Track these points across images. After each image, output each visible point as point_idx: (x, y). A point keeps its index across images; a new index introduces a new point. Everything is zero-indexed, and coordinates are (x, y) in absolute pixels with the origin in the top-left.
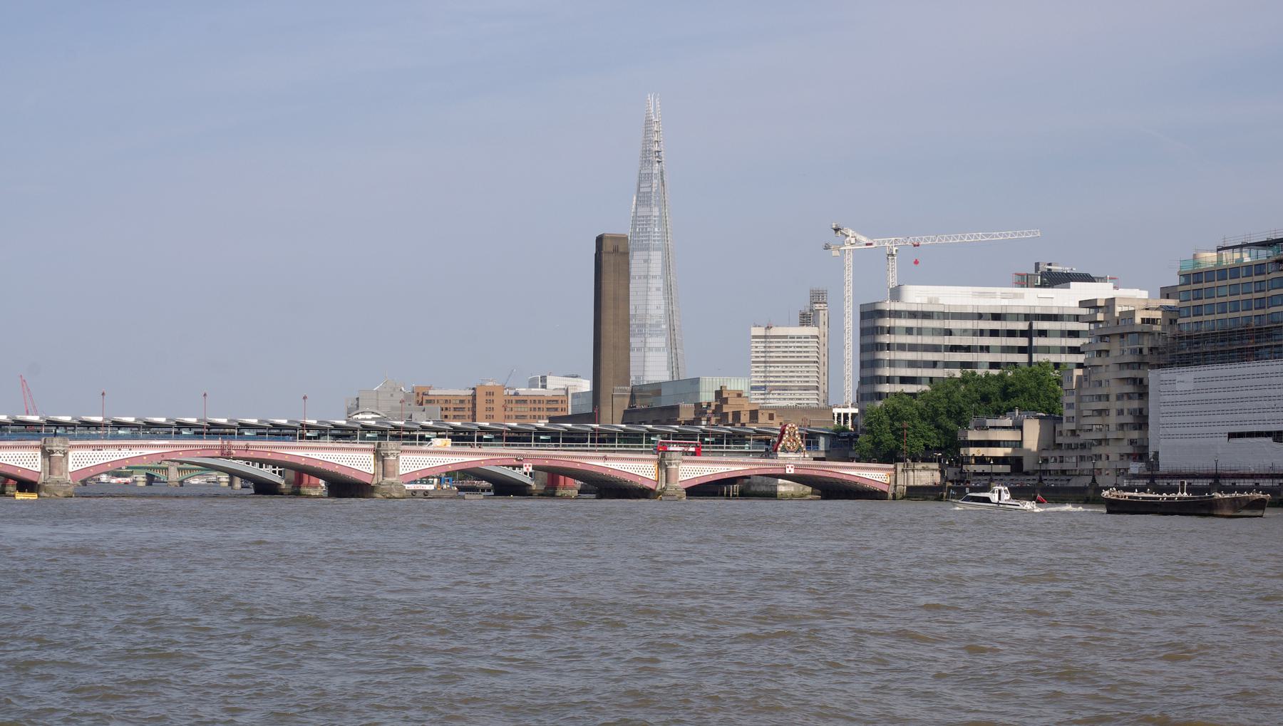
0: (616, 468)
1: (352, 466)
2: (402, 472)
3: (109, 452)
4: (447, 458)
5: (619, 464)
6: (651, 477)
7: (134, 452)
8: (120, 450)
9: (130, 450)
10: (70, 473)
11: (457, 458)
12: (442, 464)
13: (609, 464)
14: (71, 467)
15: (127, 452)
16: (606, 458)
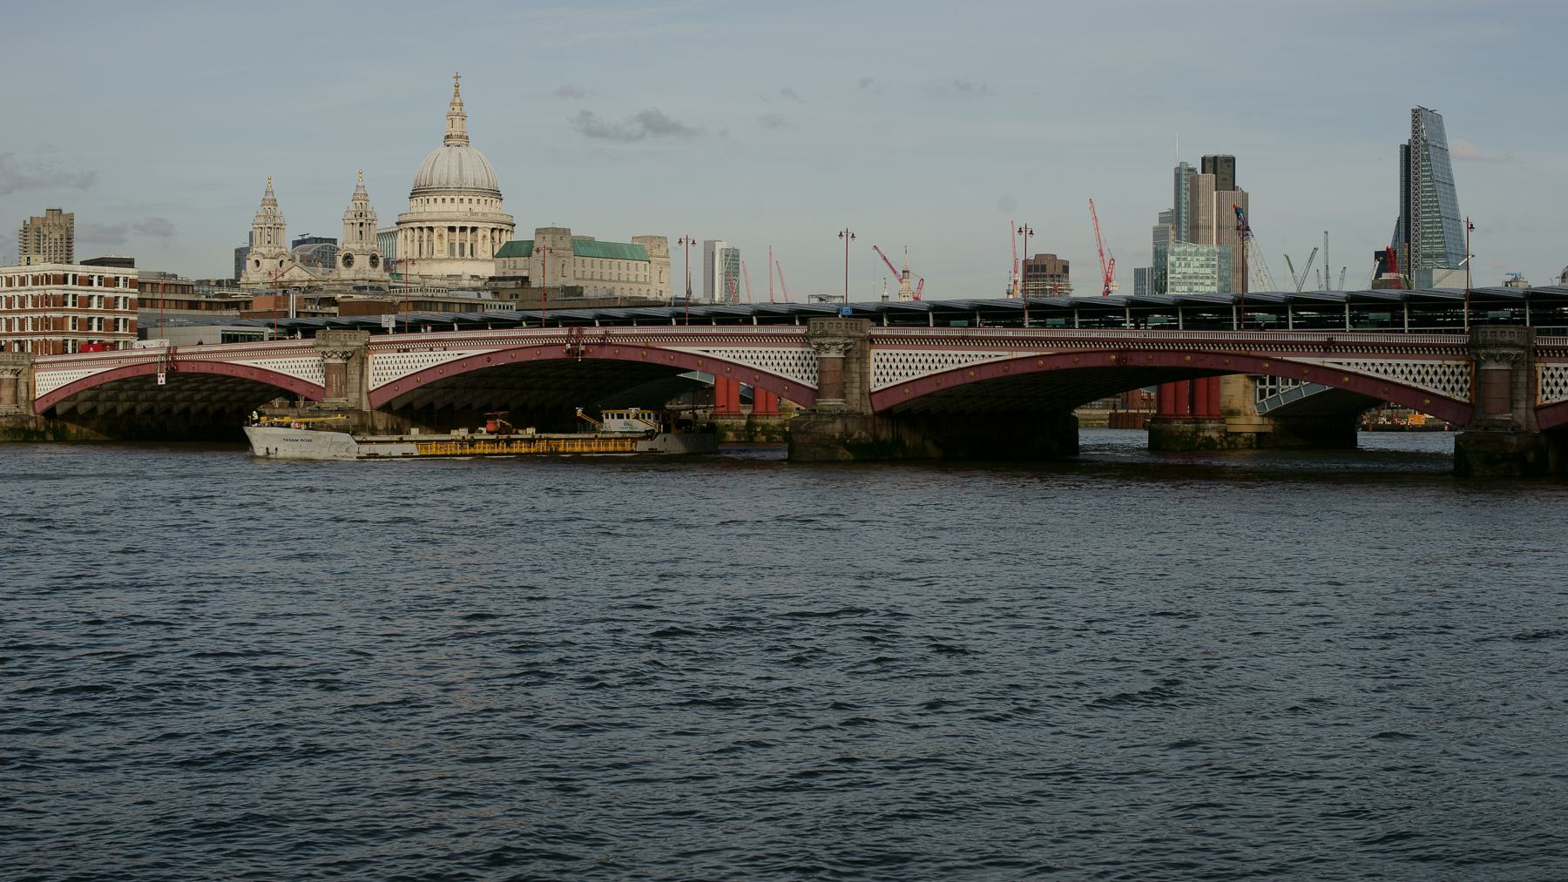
0: (1364, 371)
1: (784, 375)
2: (875, 385)
3: (419, 354)
4: (966, 353)
5: (1369, 361)
6: (1459, 397)
7: (451, 352)
8: (431, 350)
9: (445, 349)
10: (369, 393)
11: (987, 353)
12: (954, 367)
13: (1345, 361)
14: (373, 383)
15: (442, 353)
16: (1328, 347)
